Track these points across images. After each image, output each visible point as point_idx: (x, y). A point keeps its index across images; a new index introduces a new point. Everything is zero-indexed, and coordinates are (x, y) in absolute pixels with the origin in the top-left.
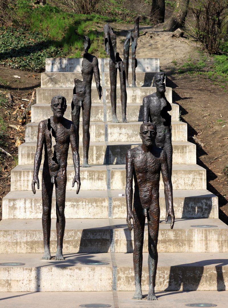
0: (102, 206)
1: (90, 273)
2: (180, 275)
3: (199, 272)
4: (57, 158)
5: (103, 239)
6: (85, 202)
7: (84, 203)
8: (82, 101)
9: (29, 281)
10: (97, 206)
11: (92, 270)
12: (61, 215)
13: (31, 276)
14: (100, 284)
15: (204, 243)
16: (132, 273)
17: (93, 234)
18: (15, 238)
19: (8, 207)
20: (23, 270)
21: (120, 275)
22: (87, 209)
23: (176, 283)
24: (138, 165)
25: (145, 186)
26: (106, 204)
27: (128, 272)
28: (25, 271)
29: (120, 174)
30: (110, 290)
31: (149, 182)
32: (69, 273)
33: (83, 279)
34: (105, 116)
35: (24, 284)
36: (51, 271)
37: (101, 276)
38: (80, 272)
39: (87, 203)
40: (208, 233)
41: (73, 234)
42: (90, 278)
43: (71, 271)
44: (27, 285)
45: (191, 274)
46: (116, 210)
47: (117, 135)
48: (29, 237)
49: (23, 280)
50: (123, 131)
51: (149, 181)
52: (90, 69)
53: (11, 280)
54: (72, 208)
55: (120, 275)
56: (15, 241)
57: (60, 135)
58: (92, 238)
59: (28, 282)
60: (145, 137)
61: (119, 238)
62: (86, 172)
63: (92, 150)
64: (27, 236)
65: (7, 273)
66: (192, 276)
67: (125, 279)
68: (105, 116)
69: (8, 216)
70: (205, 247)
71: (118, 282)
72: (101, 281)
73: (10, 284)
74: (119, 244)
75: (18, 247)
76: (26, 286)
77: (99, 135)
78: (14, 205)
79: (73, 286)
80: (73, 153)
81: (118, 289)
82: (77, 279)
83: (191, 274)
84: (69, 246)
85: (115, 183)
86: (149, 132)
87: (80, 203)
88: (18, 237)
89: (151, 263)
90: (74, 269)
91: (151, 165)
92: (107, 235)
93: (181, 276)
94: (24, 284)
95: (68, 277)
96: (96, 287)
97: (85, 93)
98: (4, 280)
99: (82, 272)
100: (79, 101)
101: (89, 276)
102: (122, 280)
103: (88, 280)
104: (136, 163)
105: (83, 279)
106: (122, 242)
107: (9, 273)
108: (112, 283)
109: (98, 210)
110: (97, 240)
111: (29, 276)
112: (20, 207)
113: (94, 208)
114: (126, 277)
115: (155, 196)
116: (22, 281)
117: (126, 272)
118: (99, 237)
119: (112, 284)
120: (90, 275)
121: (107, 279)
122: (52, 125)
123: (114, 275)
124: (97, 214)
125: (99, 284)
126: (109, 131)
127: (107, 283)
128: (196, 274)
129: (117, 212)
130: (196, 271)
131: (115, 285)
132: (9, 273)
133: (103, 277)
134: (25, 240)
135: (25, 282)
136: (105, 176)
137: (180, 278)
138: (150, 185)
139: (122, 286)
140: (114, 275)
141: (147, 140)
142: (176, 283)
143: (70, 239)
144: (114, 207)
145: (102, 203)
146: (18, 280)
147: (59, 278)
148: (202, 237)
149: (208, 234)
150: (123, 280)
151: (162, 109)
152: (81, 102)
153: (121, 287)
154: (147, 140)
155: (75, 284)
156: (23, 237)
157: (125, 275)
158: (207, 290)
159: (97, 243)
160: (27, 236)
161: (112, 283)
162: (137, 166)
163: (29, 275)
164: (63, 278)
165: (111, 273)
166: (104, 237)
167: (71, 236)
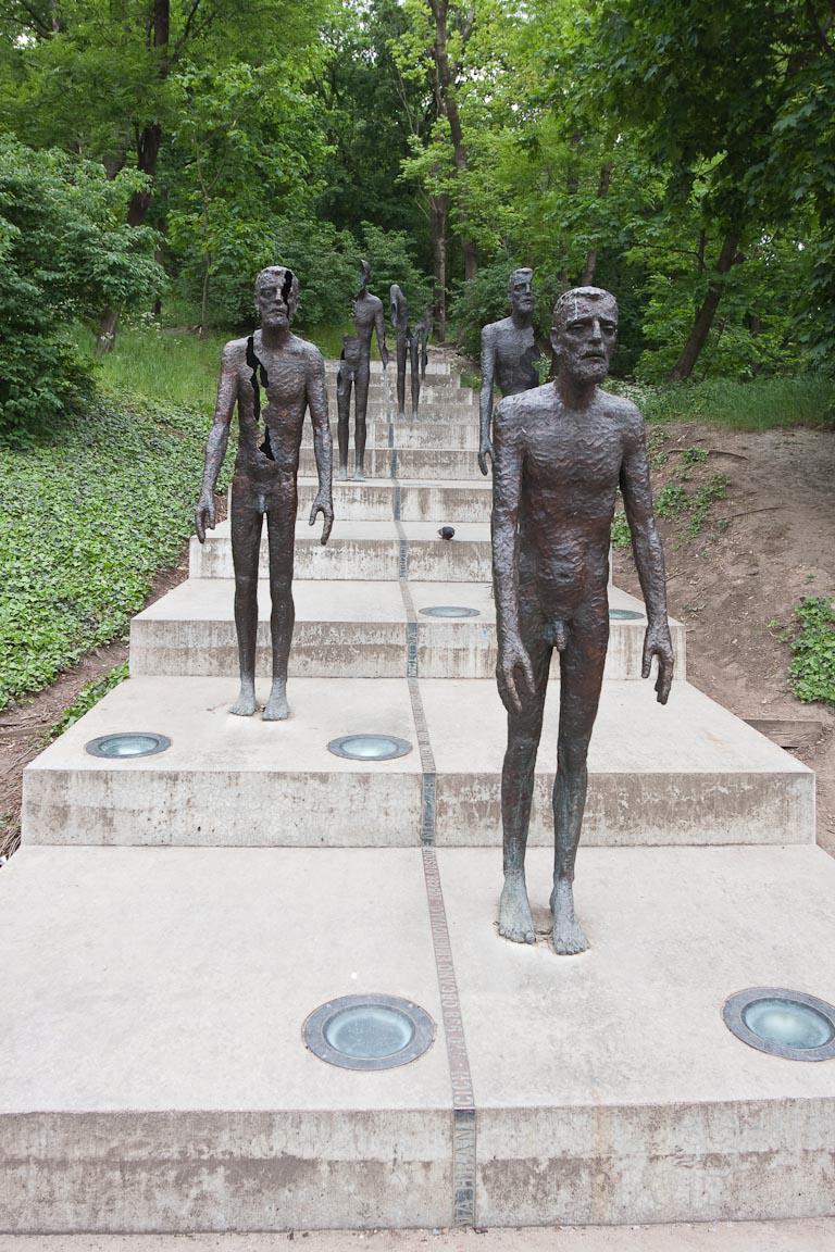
0: (387, 556)
1: (353, 791)
2: (622, 798)
3: (677, 791)
4: (273, 445)
5: (391, 646)
6: (354, 547)
7: (351, 550)
8: (356, 372)
9: (170, 812)
10: (377, 556)
11: (359, 781)
12: (282, 598)
13: (176, 799)
14: (383, 824)
15: (623, 659)
16: (480, 792)
17: (367, 634)
18: (183, 639)
19: (200, 554)
20: (152, 780)
21: (444, 798)
22: (357, 559)
23: (609, 822)
24: (541, 459)
25: (563, 536)
26: (394, 552)
27: (468, 789)
28: (155, 784)
29: (416, 493)
30: (414, 842)
31: (579, 525)
32: (289, 791)
33: (332, 811)
34: (389, 416)
35: (155, 822)
36: (237, 784)
37: (387, 800)
38: (323, 788)
39: (357, 550)
40: (632, 633)
41: (320, 632)
42: (353, 808)
43: (298, 784)
44: (164, 826)
45: (653, 796)
46: (414, 564)
47: (407, 438)
48: (214, 637)
49: (151, 810)
50: (415, 432)
51: (576, 521)
52: (369, 318)
53: (113, 809)
54: (327, 559)
55: (444, 798)
56: (182, 646)
57: (278, 381)
58: (364, 642)
59: (164, 816)
60: (578, 343)
61: (427, 644)
62: (359, 490)
63: (370, 456)
64: (210, 635)
65: (103, 787)
66: (657, 800)
67: (458, 809)
68: (389, 416)
69: (200, 571)
70: (625, 668)
71: (440, 820)
72: (386, 814)
73: (109, 822)
74: (427, 658)
75: (190, 662)
76: (158, 829)
77: (380, 438)
78: (213, 550)
79: (302, 831)
80: (315, 431)
81: (439, 840)
82: (315, 808)
83: (653, 796)
84: (309, 660)
85: (409, 510)
86: (597, 323)
87: (344, 549)
88: (190, 637)
89: (565, 806)
90: (306, 779)
91: (591, 458)
92: (401, 636)
93: (625, 803)
94: (155, 822)
95: (288, 802)
96: (371, 833)
97: (360, 358)
98: (93, 809)
99: (330, 788)
100: (350, 372)
101: (351, 800)
102: (450, 813)
103: (347, 812)
104: (535, 448)
105: (332, 811)
106: (435, 652)
107: (108, 788)
108: (420, 822)
109: (379, 563)
110: (374, 648)
111: (169, 798)
112: (225, 555)
113: (371, 559)
114: (461, 803)
115: (596, 577)
116: (146, 815)
117: (462, 790)
118: (380, 641)
119: (420, 827)
120: (355, 797)
121: (404, 811)
122: (257, 353)
123: (426, 797)
124: (376, 571)
125: (380, 825)
126: (395, 432)
127: (404, 822)
128: (670, 796)
129: (416, 568)
130: (670, 788)
131: (429, 830)
132: (108, 788)
133: (393, 803)
134: (205, 646)
135: (157, 816)
136: (390, 497)
137: (622, 807)
138: (580, 533)
139: (450, 831)
140: (427, 798)
141: (583, 358)
142: (609, 822)
143: (312, 644)
144: (410, 558)
145: (386, 549)
146: (136, 808)
147: (259, 805)
148: (620, 643)
149: (633, 638)
150: (454, 812)
151: (524, 351)
152: (353, 374)
153: (446, 834)
154: (583, 358)
155: (309, 825)
156: (201, 639)
157: (461, 799)
158: (700, 843)
159: (375, 655)
160: (210, 635)
161: (420, 822)
162: (536, 460)
163: (168, 794)
164: (272, 807)
165: (419, 792)
166: (392, 642)
167: (315, 638)
